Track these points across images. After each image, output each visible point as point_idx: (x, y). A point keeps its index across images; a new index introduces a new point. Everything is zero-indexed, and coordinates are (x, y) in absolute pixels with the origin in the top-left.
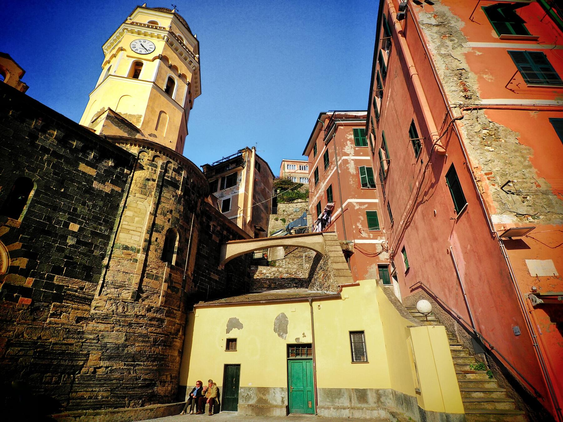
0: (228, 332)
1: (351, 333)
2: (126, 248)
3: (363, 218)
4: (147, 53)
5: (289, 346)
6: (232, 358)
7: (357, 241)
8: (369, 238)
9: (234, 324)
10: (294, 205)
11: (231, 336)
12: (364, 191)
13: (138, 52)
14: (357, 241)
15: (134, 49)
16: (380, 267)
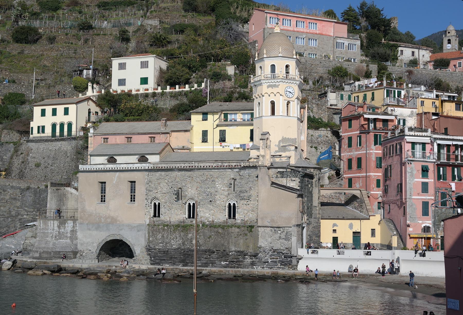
0: (333, 227)
1: (372, 229)
2: (315, 207)
3: (375, 182)
4: (292, 96)
5: (353, 232)
6: (335, 235)
7: (372, 192)
8: (376, 191)
9: (334, 225)
10: (319, 131)
11: (334, 229)
12: (377, 169)
13: (288, 97)
14: (372, 192)
15: (287, 95)
16: (378, 202)
